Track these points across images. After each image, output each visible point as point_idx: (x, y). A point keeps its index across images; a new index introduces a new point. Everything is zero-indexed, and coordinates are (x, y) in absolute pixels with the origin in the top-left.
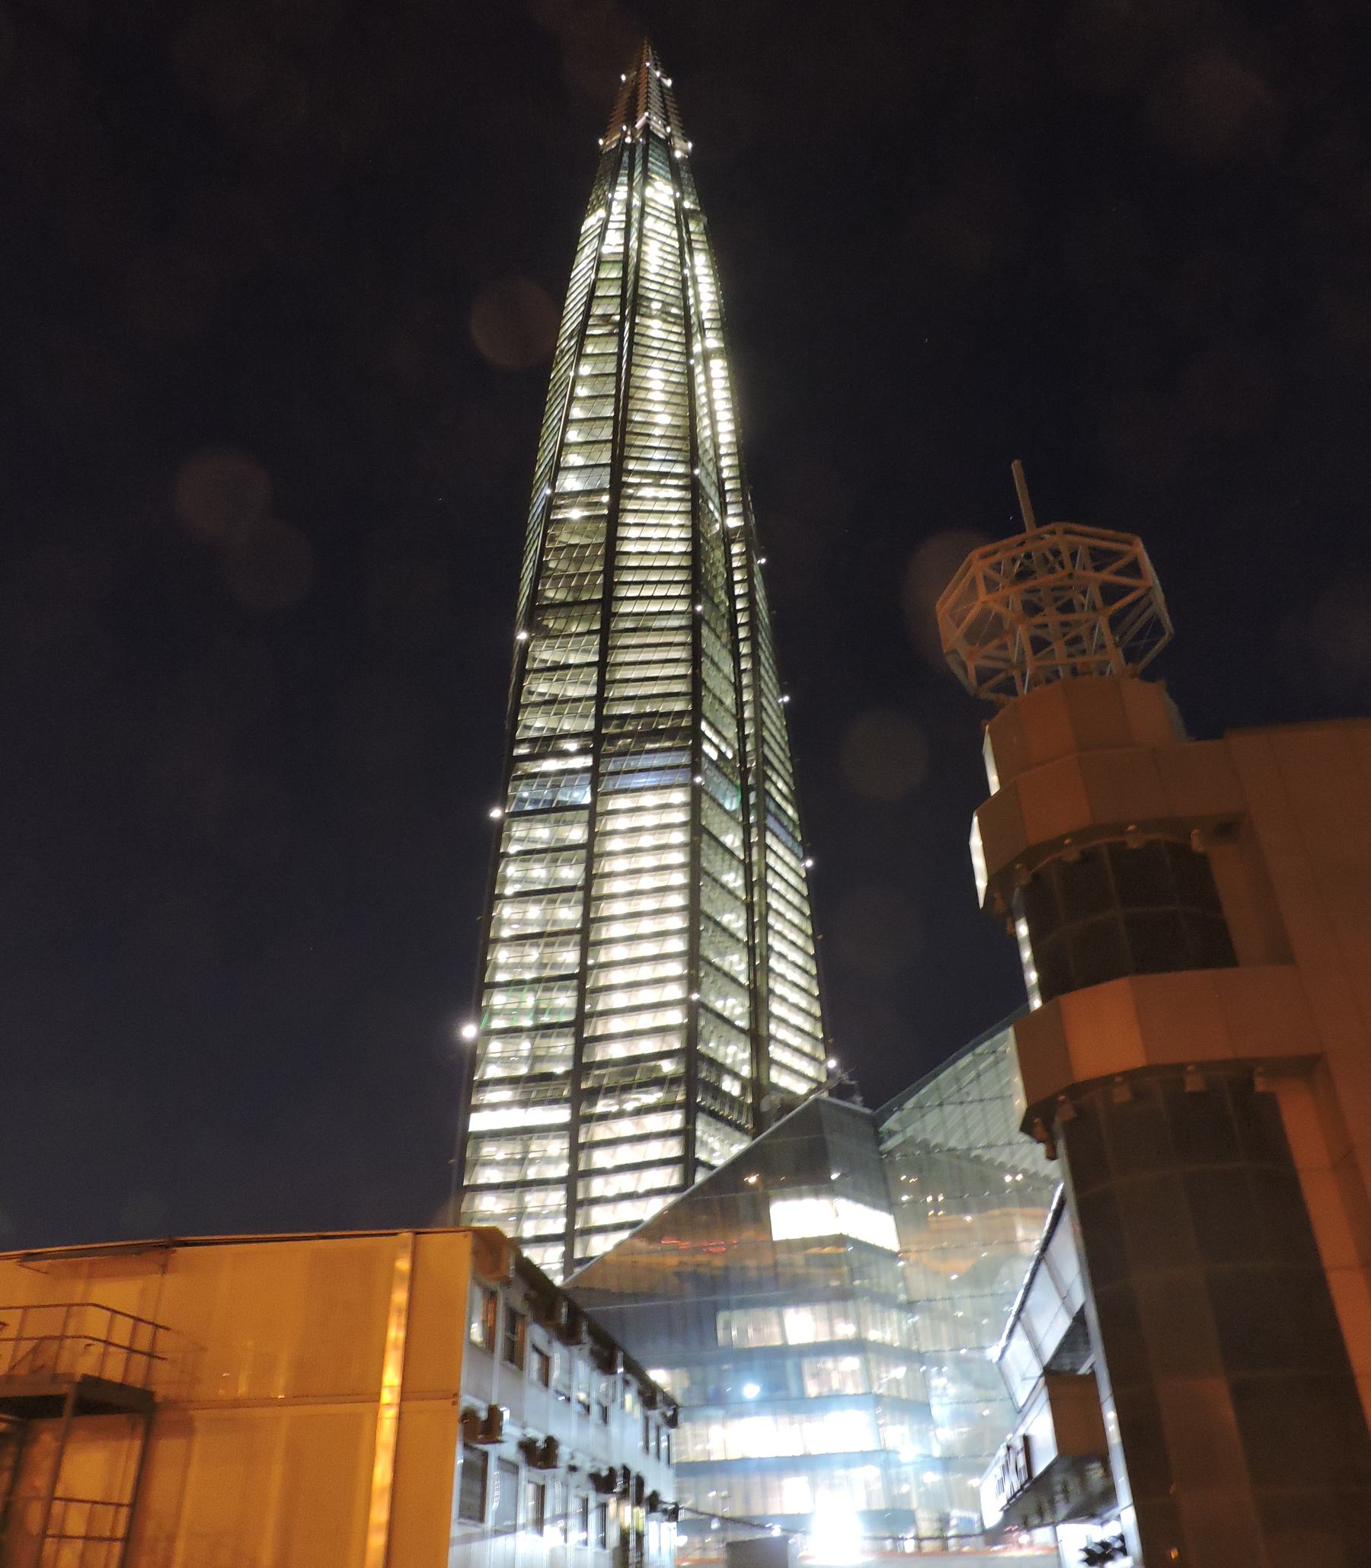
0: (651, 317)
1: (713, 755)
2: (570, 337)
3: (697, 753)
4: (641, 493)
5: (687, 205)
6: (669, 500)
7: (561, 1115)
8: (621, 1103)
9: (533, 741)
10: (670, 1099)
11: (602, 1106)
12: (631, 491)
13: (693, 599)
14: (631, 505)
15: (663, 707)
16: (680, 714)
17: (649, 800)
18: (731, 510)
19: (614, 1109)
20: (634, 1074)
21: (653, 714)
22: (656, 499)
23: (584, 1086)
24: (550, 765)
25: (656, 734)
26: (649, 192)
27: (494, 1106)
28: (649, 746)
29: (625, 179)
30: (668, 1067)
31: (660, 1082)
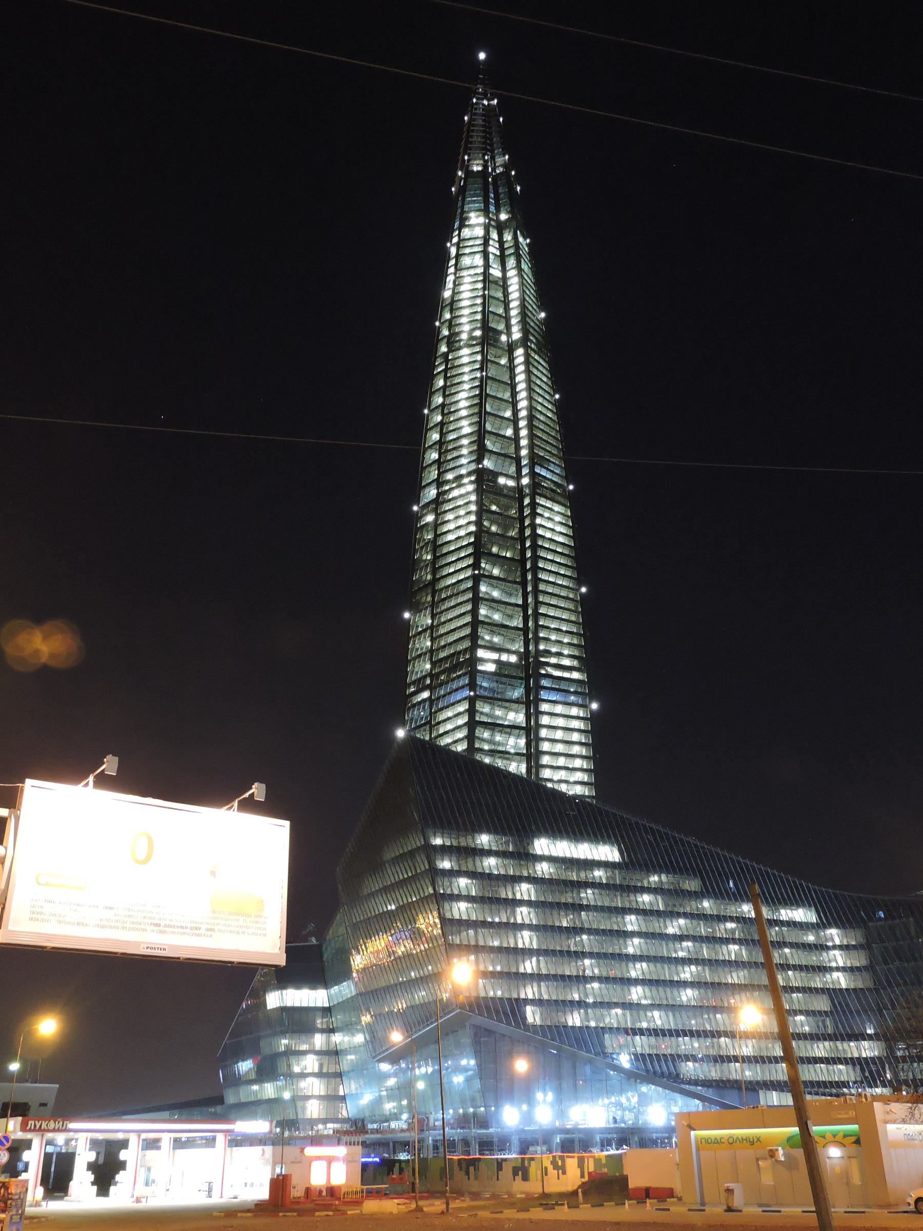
0: (459, 348)
1: (491, 668)
3: (473, 674)
4: (450, 497)
5: (503, 217)
6: (468, 493)
9: (414, 683)
13: (476, 565)
14: (447, 507)
15: (461, 647)
16: (465, 650)
18: (525, 471)
21: (453, 655)
22: (461, 496)
25: (454, 668)
26: (466, 233)
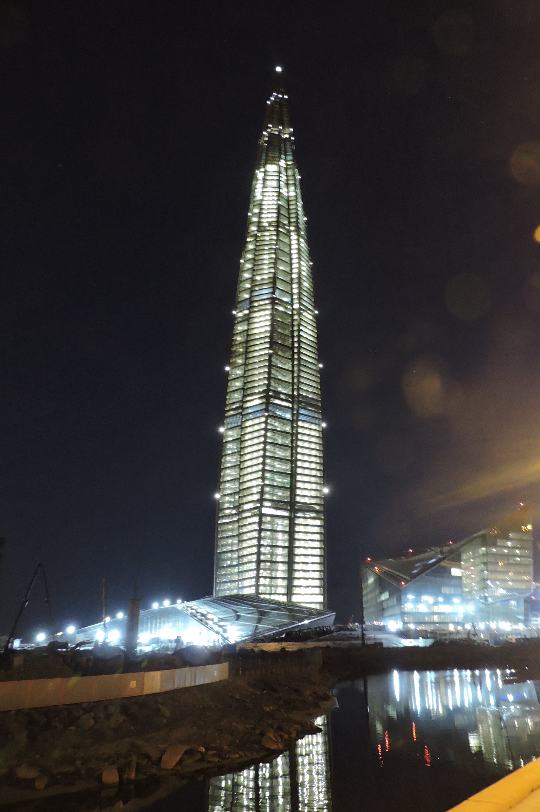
2: (270, 224)
7: (286, 514)
8: (304, 514)
10: (318, 516)
11: (300, 514)
12: (301, 311)
17: (306, 425)
19: (302, 515)
20: (307, 508)
23: (293, 507)
24: (277, 402)
25: (312, 406)
27: (266, 507)
28: (309, 408)
29: (283, 156)
30: (317, 507)
31: (317, 512)
